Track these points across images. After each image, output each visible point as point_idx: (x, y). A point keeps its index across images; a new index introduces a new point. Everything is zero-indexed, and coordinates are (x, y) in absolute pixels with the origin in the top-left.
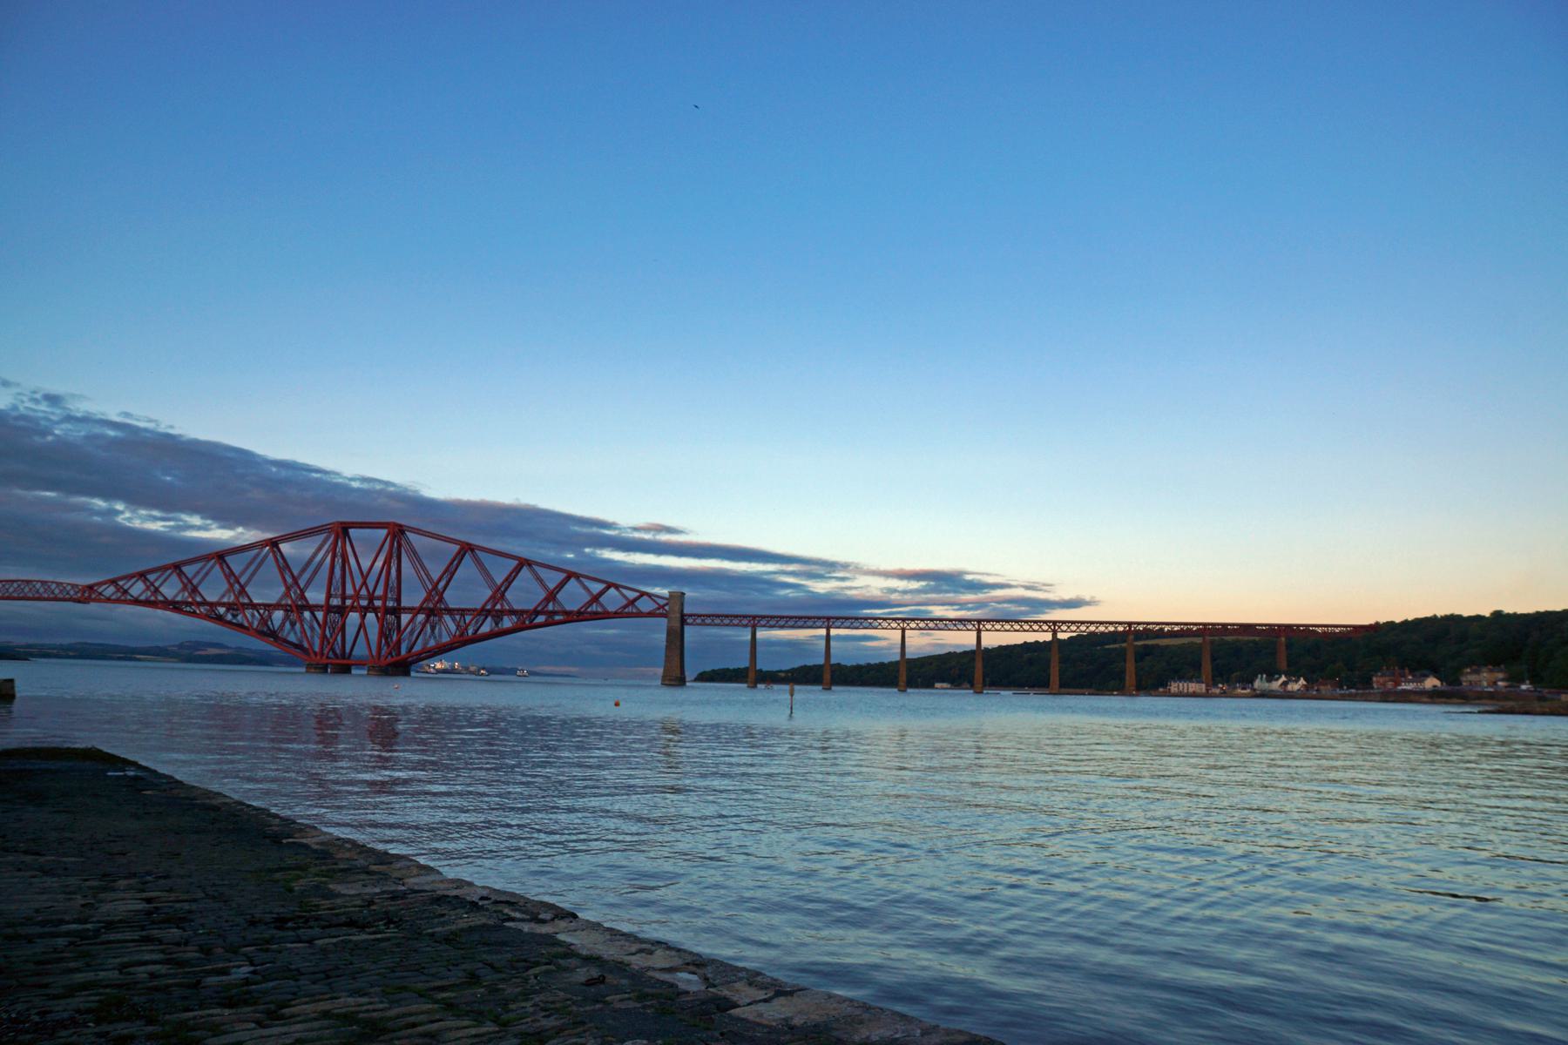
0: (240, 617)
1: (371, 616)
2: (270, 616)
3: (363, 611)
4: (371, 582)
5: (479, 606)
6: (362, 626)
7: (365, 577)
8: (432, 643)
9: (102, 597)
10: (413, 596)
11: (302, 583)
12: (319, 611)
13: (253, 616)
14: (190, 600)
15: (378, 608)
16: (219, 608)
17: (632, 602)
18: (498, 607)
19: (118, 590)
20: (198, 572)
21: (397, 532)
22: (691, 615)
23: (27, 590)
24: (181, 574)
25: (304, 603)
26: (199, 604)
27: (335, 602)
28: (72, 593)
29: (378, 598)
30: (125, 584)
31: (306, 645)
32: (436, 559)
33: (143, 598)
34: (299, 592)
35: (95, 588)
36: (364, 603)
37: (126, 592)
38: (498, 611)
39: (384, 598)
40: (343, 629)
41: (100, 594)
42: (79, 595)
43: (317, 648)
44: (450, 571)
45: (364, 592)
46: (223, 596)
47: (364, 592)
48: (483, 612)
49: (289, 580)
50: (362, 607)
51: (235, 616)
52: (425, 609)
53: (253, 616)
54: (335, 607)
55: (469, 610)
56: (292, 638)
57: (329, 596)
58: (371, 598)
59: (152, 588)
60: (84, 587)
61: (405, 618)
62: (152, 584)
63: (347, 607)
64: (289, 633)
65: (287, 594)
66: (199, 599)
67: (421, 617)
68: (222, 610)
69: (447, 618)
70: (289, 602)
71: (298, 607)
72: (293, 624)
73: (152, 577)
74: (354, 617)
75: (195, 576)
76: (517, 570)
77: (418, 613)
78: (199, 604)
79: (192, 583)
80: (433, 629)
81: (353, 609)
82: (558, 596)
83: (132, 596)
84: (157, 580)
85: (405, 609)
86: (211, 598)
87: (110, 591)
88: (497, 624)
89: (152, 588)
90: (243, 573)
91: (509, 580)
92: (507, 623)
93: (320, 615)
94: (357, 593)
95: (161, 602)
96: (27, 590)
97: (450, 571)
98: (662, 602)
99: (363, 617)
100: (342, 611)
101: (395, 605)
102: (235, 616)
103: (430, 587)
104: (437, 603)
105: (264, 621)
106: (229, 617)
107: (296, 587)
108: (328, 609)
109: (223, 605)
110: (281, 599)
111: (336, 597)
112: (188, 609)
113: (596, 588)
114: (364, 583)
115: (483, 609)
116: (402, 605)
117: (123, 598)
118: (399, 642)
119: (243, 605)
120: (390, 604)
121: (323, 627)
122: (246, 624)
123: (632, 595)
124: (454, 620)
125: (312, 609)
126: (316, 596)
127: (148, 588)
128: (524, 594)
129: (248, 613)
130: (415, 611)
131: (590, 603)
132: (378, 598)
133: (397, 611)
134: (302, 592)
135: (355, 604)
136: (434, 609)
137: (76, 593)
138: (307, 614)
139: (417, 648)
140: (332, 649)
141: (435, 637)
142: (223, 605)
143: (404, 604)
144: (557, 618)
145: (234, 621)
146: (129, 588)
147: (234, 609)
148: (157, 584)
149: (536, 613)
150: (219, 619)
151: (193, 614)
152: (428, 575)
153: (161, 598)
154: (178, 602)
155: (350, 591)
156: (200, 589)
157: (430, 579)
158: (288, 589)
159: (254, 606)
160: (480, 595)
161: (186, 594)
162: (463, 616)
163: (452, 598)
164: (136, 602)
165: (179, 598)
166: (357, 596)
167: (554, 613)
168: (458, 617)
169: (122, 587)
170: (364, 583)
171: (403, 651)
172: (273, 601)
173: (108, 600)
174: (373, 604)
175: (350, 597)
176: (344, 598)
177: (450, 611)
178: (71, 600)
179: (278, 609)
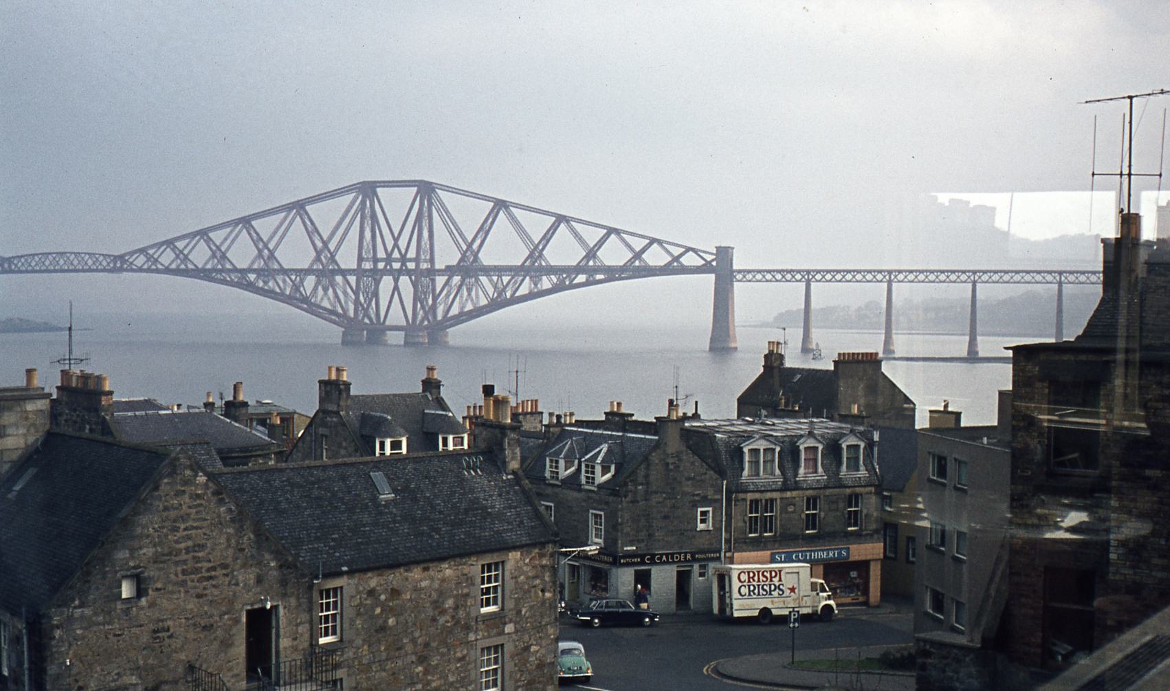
0: (271, 284)
1: (404, 281)
2: (302, 281)
3: (396, 275)
4: (402, 243)
6: (396, 288)
7: (396, 240)
8: (469, 307)
10: (447, 254)
11: (332, 246)
12: (351, 275)
13: (284, 281)
14: (220, 267)
15: (412, 270)
17: (677, 259)
19: (148, 260)
20: (226, 239)
21: (426, 190)
22: (739, 271)
23: (62, 262)
24: (209, 241)
25: (336, 267)
26: (229, 271)
27: (367, 265)
29: (411, 260)
30: (154, 253)
31: (340, 311)
32: (469, 215)
33: (173, 266)
34: (329, 256)
35: (127, 258)
36: (396, 266)
37: (156, 260)
39: (417, 260)
40: (376, 294)
41: (131, 263)
43: (351, 314)
44: (484, 230)
45: (396, 255)
46: (253, 263)
47: (396, 255)
49: (319, 244)
51: (266, 283)
53: (284, 281)
54: (366, 271)
56: (326, 304)
57: (360, 259)
58: (403, 259)
59: (181, 256)
61: (440, 281)
62: (181, 252)
63: (381, 270)
64: (322, 299)
65: (318, 259)
67: (456, 279)
68: (252, 277)
69: (484, 279)
71: (327, 272)
72: (325, 290)
73: (180, 245)
74: (387, 282)
75: (223, 243)
76: (553, 229)
79: (220, 250)
80: (469, 290)
81: (385, 272)
82: (598, 253)
83: (162, 265)
84: (185, 247)
86: (242, 264)
87: (140, 261)
88: (536, 285)
90: (271, 238)
91: (547, 238)
92: (546, 283)
93: (352, 279)
94: (389, 255)
95: (192, 270)
96: (62, 262)
97: (484, 230)
98: (709, 258)
99: (396, 281)
100: (376, 275)
102: (266, 283)
103: (464, 247)
104: (472, 262)
105: (296, 288)
106: (261, 284)
107: (326, 252)
108: (359, 272)
109: (254, 271)
110: (312, 264)
111: (367, 260)
112: (219, 276)
113: (638, 244)
114: (396, 245)
117: (153, 267)
118: (434, 308)
119: (274, 270)
120: (424, 266)
121: (356, 293)
122: (278, 290)
123: (676, 251)
124: (491, 281)
125: (344, 273)
126: (347, 258)
127: (177, 256)
128: (564, 252)
129: (279, 278)
130: (450, 271)
131: (631, 261)
132: (411, 260)
133: (432, 272)
134: (333, 256)
135: (388, 267)
136: (469, 268)
137: (108, 264)
138: (339, 279)
139: (455, 311)
140: (367, 315)
141: (472, 300)
142: (254, 271)
143: (437, 266)
144: (599, 277)
145: (266, 288)
146: (159, 256)
147: (265, 276)
148: (186, 252)
149: (578, 269)
150: (250, 287)
151: (224, 282)
152: (461, 234)
153: (190, 266)
154: (209, 270)
155: (381, 254)
156: (228, 255)
157: (464, 239)
158: (318, 253)
159: (286, 272)
160: (517, 256)
161: (216, 261)
162: (500, 276)
163: (486, 258)
164: (167, 271)
165: (209, 266)
166: (388, 259)
167: (597, 270)
168: (495, 278)
169: (152, 256)
170: (396, 245)
171: (439, 317)
173: (140, 270)
174: (406, 267)
175: (382, 260)
177: (487, 271)
178: (104, 270)
179: (310, 275)
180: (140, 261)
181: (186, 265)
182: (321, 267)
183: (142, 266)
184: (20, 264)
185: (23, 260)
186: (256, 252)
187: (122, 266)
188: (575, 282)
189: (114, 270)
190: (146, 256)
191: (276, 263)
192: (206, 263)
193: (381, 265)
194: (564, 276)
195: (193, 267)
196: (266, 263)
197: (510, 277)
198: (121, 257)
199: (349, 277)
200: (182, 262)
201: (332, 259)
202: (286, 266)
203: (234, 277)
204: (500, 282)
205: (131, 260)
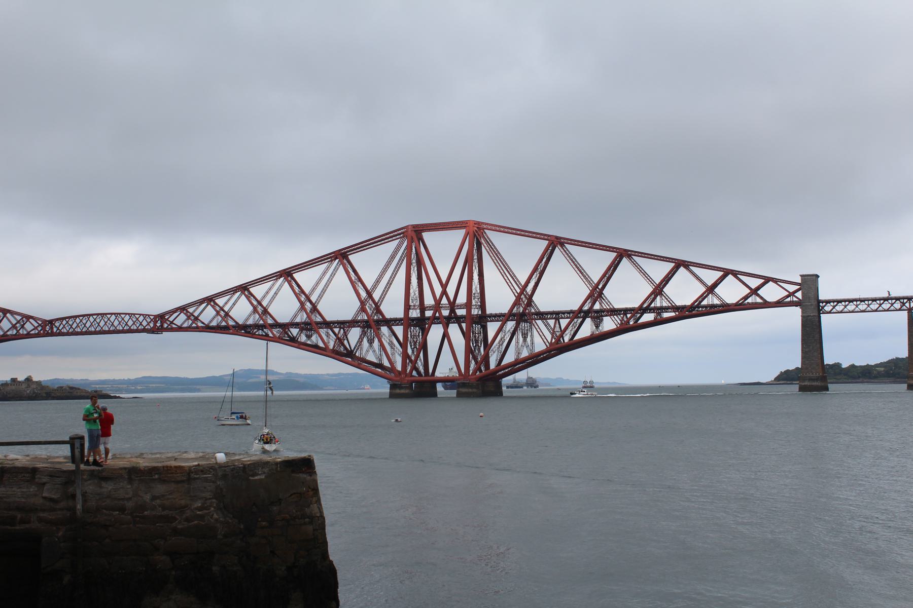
5: (576, 307)
9: (174, 326)
12: (397, 325)
14: (261, 322)
16: (291, 330)
18: (597, 306)
28: (145, 323)
33: (214, 324)
35: (166, 317)
36: (446, 313)
37: (196, 318)
38: (597, 312)
41: (172, 322)
42: (152, 325)
48: (580, 314)
50: (445, 318)
52: (514, 315)
54: (413, 319)
55: (563, 313)
59: (222, 313)
60: (155, 316)
63: (429, 318)
66: (270, 321)
70: (366, 318)
77: (508, 320)
78: (272, 326)
81: (435, 320)
85: (491, 316)
89: (222, 313)
96: (102, 324)
99: (446, 327)
100: (423, 324)
101: (480, 313)
110: (357, 315)
115: (580, 310)
116: (488, 312)
117: (194, 325)
120: (475, 312)
125: (390, 323)
130: (503, 318)
131: (703, 297)
133: (483, 319)
135: (437, 315)
137: (148, 324)
143: (489, 310)
148: (196, 314)
153: (231, 323)
154: (250, 326)
162: (557, 320)
164: (208, 328)
168: (552, 322)
172: (349, 317)
173: (180, 329)
176: (423, 308)
178: (144, 330)
179: (354, 327)
180: (181, 319)
181: (226, 322)
182: (366, 318)
183: (181, 325)
184: (62, 326)
185: (64, 322)
186: (251, 308)
187: (162, 325)
188: (640, 321)
189: (154, 331)
190: (186, 315)
191: (318, 316)
192: (247, 319)
193: (429, 314)
194: (629, 316)
195: (234, 324)
196: (308, 316)
197: (568, 320)
198: (162, 317)
199: (395, 328)
200: (223, 319)
201: (378, 310)
202: (328, 319)
203: (276, 332)
204: (557, 325)
205: (171, 319)
